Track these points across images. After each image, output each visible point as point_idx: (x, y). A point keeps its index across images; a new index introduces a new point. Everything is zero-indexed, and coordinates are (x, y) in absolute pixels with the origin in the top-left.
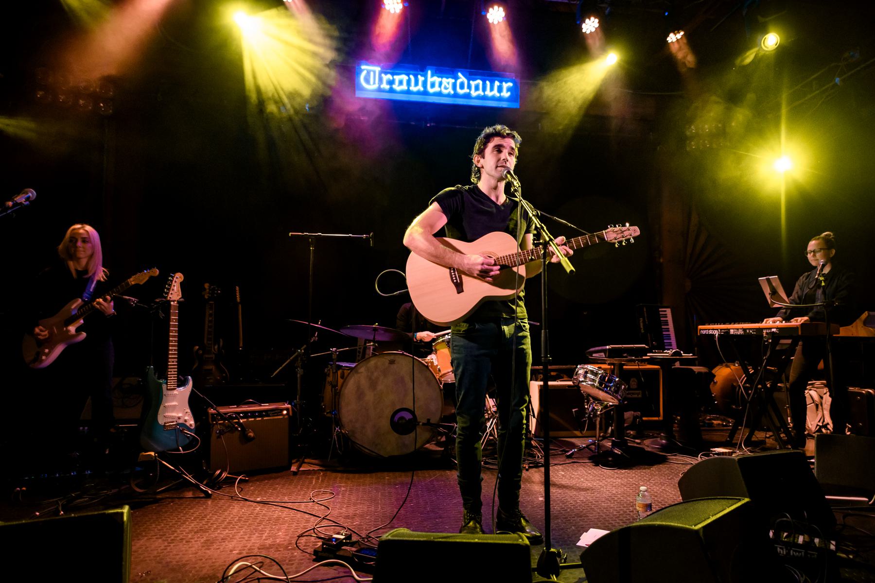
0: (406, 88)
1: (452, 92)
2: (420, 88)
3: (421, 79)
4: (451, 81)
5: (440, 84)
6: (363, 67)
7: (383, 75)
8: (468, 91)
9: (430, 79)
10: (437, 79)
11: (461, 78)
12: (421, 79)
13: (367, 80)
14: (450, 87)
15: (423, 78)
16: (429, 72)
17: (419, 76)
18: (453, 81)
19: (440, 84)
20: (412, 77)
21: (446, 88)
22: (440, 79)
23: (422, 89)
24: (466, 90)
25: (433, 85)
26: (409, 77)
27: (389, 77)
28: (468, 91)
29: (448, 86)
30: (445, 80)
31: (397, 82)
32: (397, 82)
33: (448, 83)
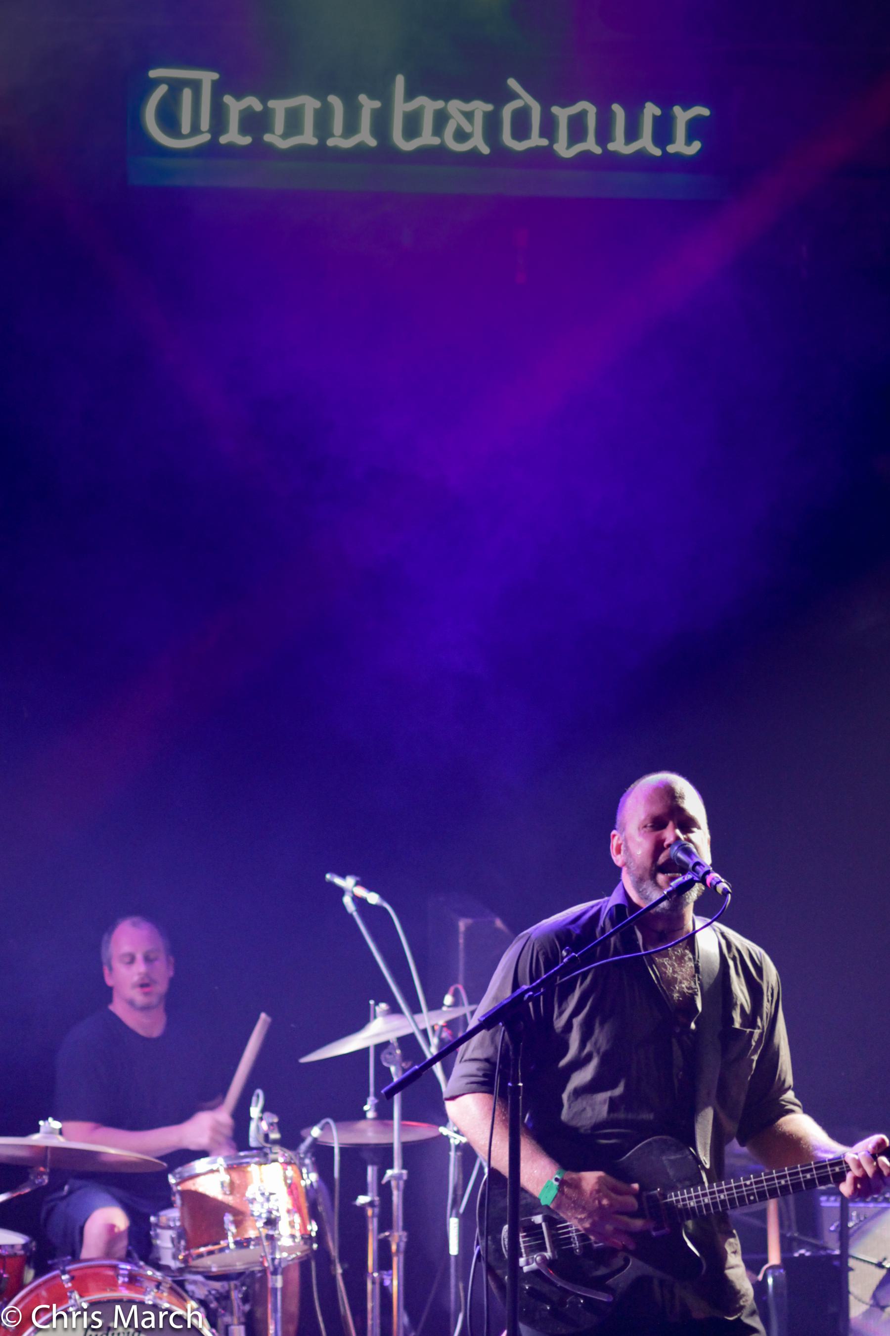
0: (314, 142)
1: (485, 150)
2: (366, 137)
3: (368, 105)
4: (480, 107)
5: (441, 119)
6: (153, 74)
7: (228, 99)
8: (544, 142)
9: (401, 107)
10: (429, 106)
11: (514, 96)
12: (368, 105)
13: (169, 121)
14: (477, 129)
15: (377, 104)
16: (400, 81)
17: (363, 98)
18: (489, 107)
19: (441, 119)
20: (335, 101)
21: (461, 136)
22: (440, 104)
23: (373, 143)
24: (536, 140)
25: (412, 127)
26: (322, 97)
27: (253, 103)
28: (544, 142)
29: (467, 128)
30: (455, 106)
31: (279, 124)
32: (279, 124)
33: (469, 116)
